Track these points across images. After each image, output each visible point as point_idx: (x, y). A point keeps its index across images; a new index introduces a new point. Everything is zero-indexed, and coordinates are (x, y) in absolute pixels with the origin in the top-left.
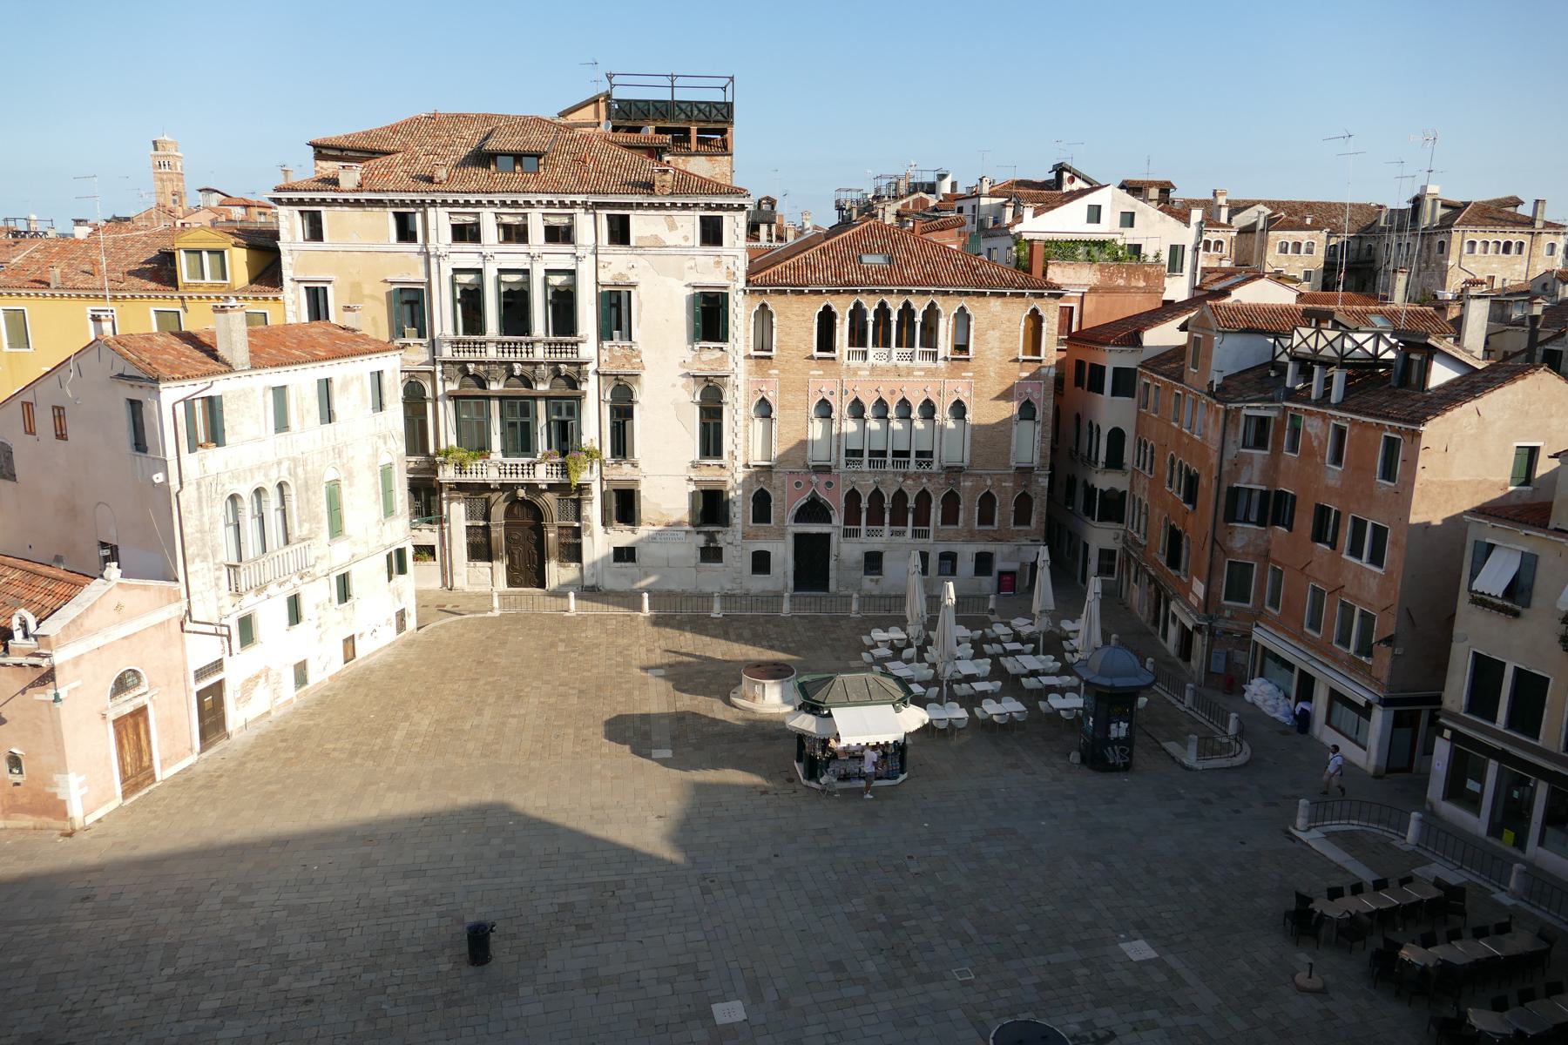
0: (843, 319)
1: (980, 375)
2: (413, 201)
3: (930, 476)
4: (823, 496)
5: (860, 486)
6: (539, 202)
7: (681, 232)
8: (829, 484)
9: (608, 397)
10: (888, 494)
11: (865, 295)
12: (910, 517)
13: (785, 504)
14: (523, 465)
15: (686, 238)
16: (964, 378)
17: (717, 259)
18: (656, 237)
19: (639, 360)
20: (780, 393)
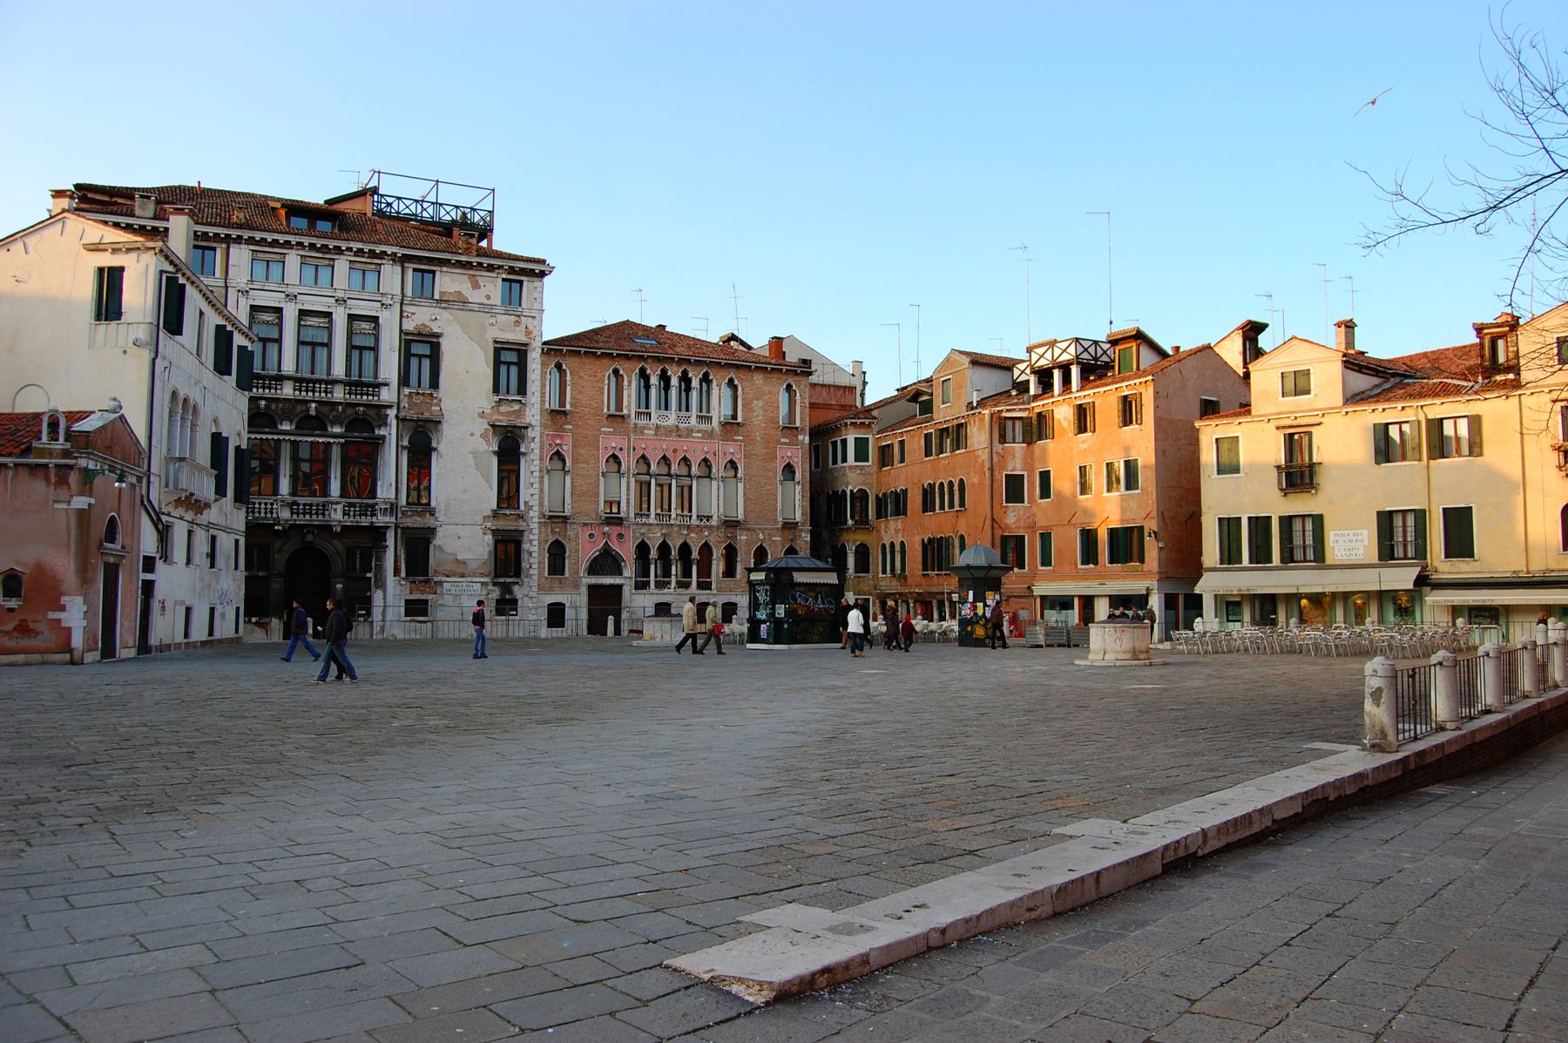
0: (630, 382)
1: (748, 440)
2: (217, 235)
4: (615, 546)
5: (649, 538)
6: (350, 249)
7: (483, 292)
8: (620, 536)
9: (406, 443)
10: (675, 545)
12: (694, 568)
13: (582, 550)
14: (318, 505)
15: (488, 297)
16: (736, 441)
17: (517, 319)
18: (459, 293)
19: (439, 409)
20: (573, 446)
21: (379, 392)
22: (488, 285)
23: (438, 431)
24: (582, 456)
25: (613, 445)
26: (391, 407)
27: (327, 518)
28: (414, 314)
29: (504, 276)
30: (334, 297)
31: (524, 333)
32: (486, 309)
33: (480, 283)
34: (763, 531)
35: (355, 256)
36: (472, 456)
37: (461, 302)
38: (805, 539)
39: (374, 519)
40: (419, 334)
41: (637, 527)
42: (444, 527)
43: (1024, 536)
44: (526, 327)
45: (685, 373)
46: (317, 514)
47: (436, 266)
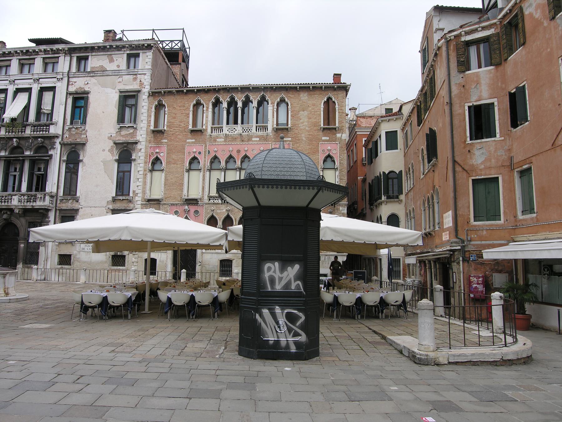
0: (208, 108)
1: (296, 140)
5: (217, 214)
7: (116, 63)
11: (222, 92)
15: (118, 66)
17: (135, 76)
20: (168, 153)
21: (49, 129)
22: (119, 59)
23: (84, 150)
24: (173, 159)
25: (195, 150)
26: (57, 137)
27: (10, 204)
28: (75, 82)
29: (128, 52)
30: (32, 79)
31: (138, 85)
32: (117, 73)
33: (114, 59)
35: (45, 54)
36: (103, 163)
37: (102, 72)
38: (342, 212)
39: (34, 204)
40: (77, 93)
41: (209, 205)
42: (84, 209)
43: (497, 178)
44: (141, 81)
45: (247, 98)
46: (5, 202)
47: (89, 53)
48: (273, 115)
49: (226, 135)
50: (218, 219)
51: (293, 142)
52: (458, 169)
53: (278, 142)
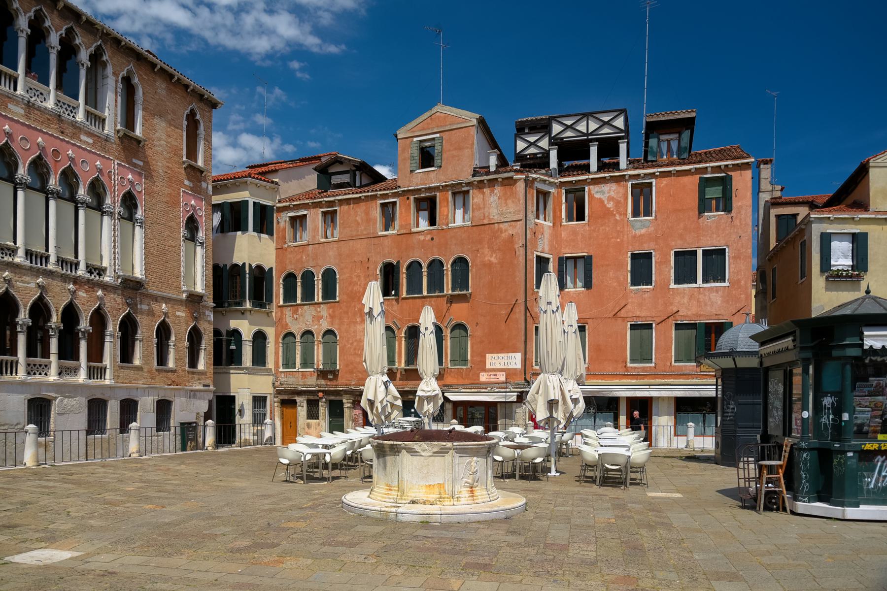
3: (105, 287)
12: (83, 346)
16: (135, 165)
34: (167, 300)
48: (116, 101)
49: (29, 102)
50: (20, 302)
51: (145, 171)
52: (528, 314)
53: (123, 161)
